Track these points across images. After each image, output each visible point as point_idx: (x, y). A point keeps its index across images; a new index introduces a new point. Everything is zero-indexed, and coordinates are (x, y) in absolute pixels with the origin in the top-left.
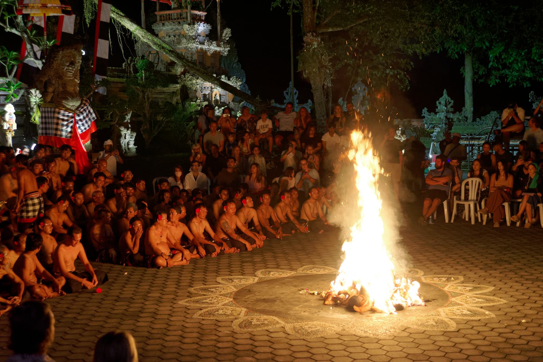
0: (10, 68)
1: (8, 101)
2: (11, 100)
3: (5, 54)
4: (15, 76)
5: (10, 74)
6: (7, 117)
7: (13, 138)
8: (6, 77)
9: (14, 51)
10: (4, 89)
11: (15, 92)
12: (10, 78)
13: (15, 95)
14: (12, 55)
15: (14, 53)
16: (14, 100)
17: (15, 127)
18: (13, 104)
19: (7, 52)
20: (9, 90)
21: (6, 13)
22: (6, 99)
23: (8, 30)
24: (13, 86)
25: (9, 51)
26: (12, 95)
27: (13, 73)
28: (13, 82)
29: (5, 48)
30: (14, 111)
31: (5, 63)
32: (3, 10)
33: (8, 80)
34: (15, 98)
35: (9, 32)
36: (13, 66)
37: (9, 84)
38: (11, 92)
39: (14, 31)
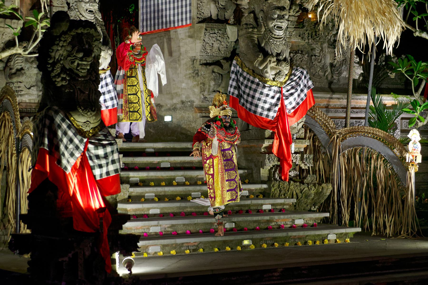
0: (417, 83)
1: (412, 125)
2: (417, 124)
3: (411, 65)
4: (422, 94)
5: (416, 91)
6: (411, 146)
7: (416, 173)
8: (412, 94)
9: (423, 62)
10: (409, 110)
11: (422, 114)
12: (417, 96)
13: (421, 118)
14: (420, 66)
15: (423, 64)
16: (420, 124)
17: (419, 160)
18: (418, 129)
19: (413, 62)
20: (413, 112)
21: (416, 13)
22: (410, 123)
23: (417, 34)
24: (420, 106)
25: (417, 62)
26: (418, 119)
27: (421, 90)
28: (420, 102)
29: (412, 58)
30: (420, 139)
31: (411, 77)
32: (413, 9)
33: (413, 99)
34: (421, 122)
35: (417, 36)
36: (421, 80)
37: (414, 104)
38: (417, 114)
39: (424, 35)
